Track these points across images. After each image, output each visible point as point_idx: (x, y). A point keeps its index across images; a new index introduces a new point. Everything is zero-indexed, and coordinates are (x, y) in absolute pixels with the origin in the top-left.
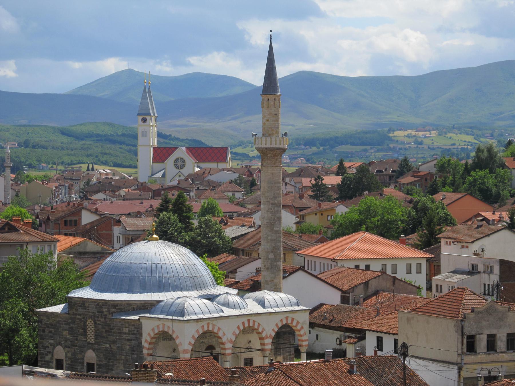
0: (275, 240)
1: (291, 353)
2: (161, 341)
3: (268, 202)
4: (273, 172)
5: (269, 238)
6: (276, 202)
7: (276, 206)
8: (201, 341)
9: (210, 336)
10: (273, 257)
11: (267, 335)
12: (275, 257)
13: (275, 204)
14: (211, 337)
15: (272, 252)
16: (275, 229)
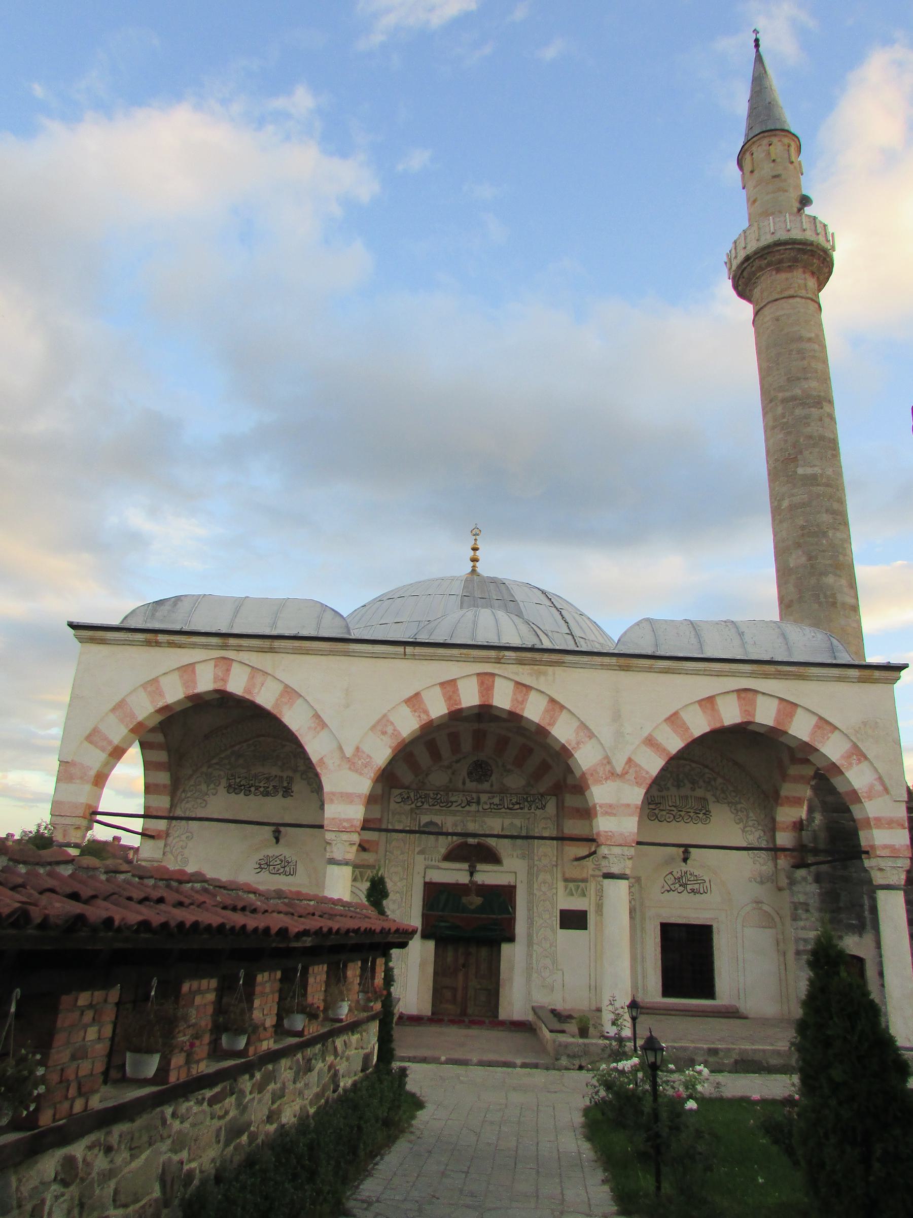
0: (803, 505)
1: (841, 904)
2: (222, 790)
3: (771, 401)
4: (778, 314)
5: (785, 504)
6: (798, 392)
7: (801, 404)
8: (425, 819)
9: (469, 803)
10: (803, 560)
11: (608, 760)
12: (810, 558)
13: (794, 398)
14: (474, 808)
15: (798, 545)
16: (800, 471)
